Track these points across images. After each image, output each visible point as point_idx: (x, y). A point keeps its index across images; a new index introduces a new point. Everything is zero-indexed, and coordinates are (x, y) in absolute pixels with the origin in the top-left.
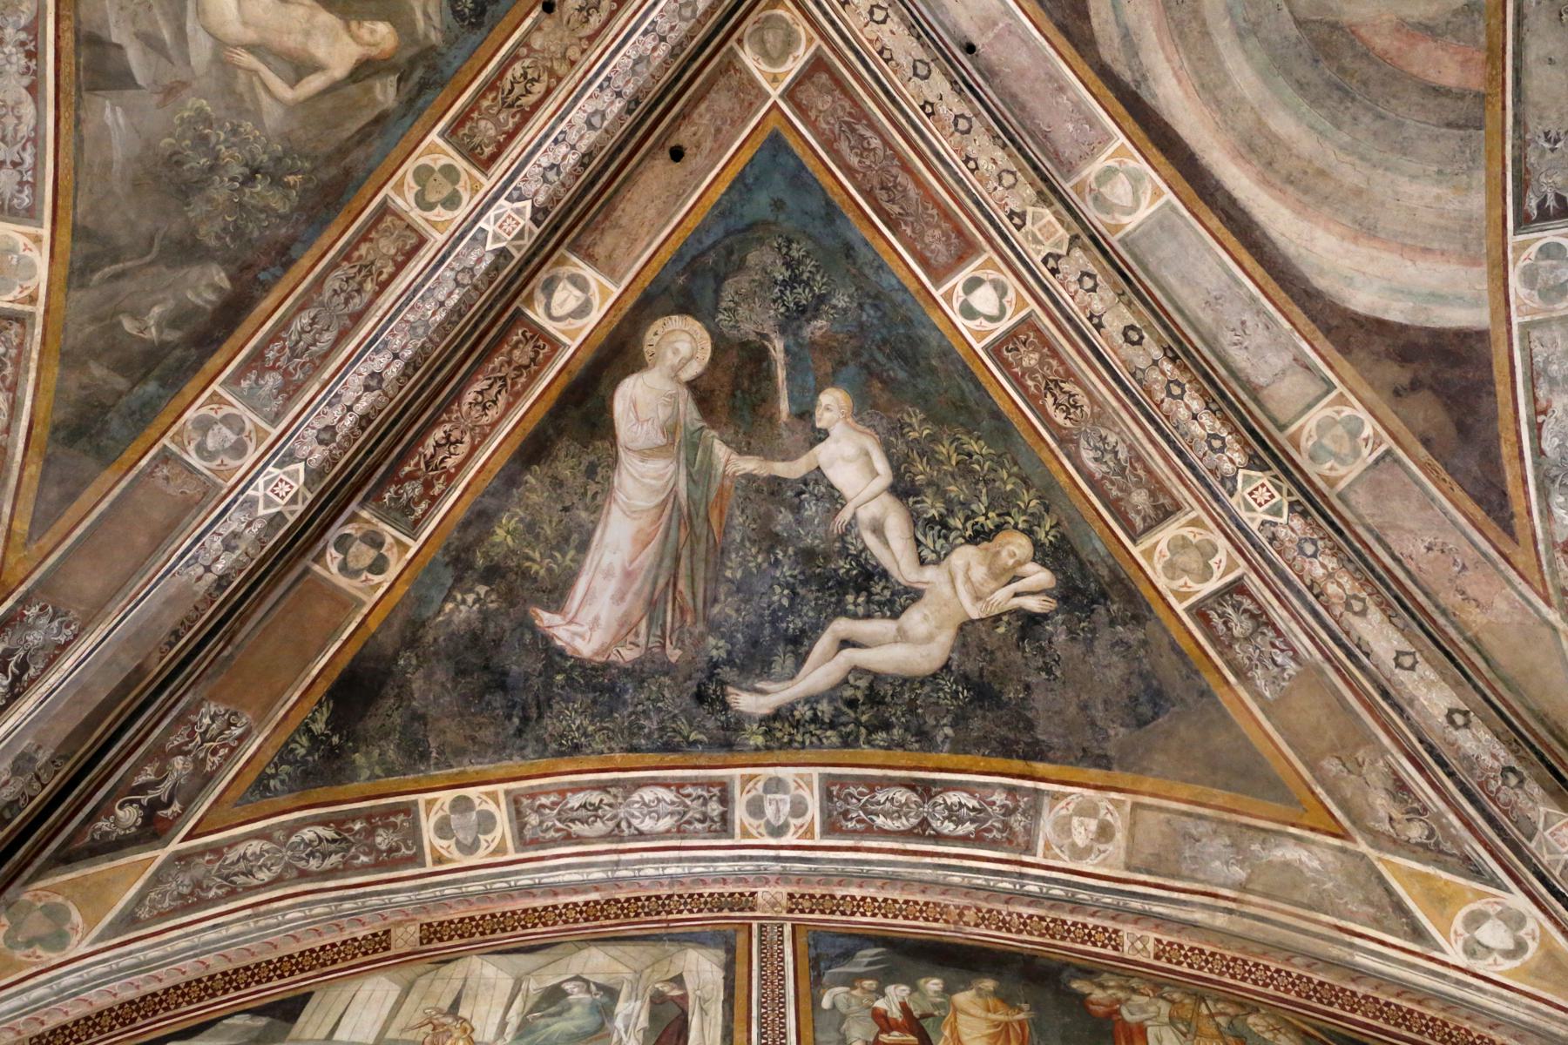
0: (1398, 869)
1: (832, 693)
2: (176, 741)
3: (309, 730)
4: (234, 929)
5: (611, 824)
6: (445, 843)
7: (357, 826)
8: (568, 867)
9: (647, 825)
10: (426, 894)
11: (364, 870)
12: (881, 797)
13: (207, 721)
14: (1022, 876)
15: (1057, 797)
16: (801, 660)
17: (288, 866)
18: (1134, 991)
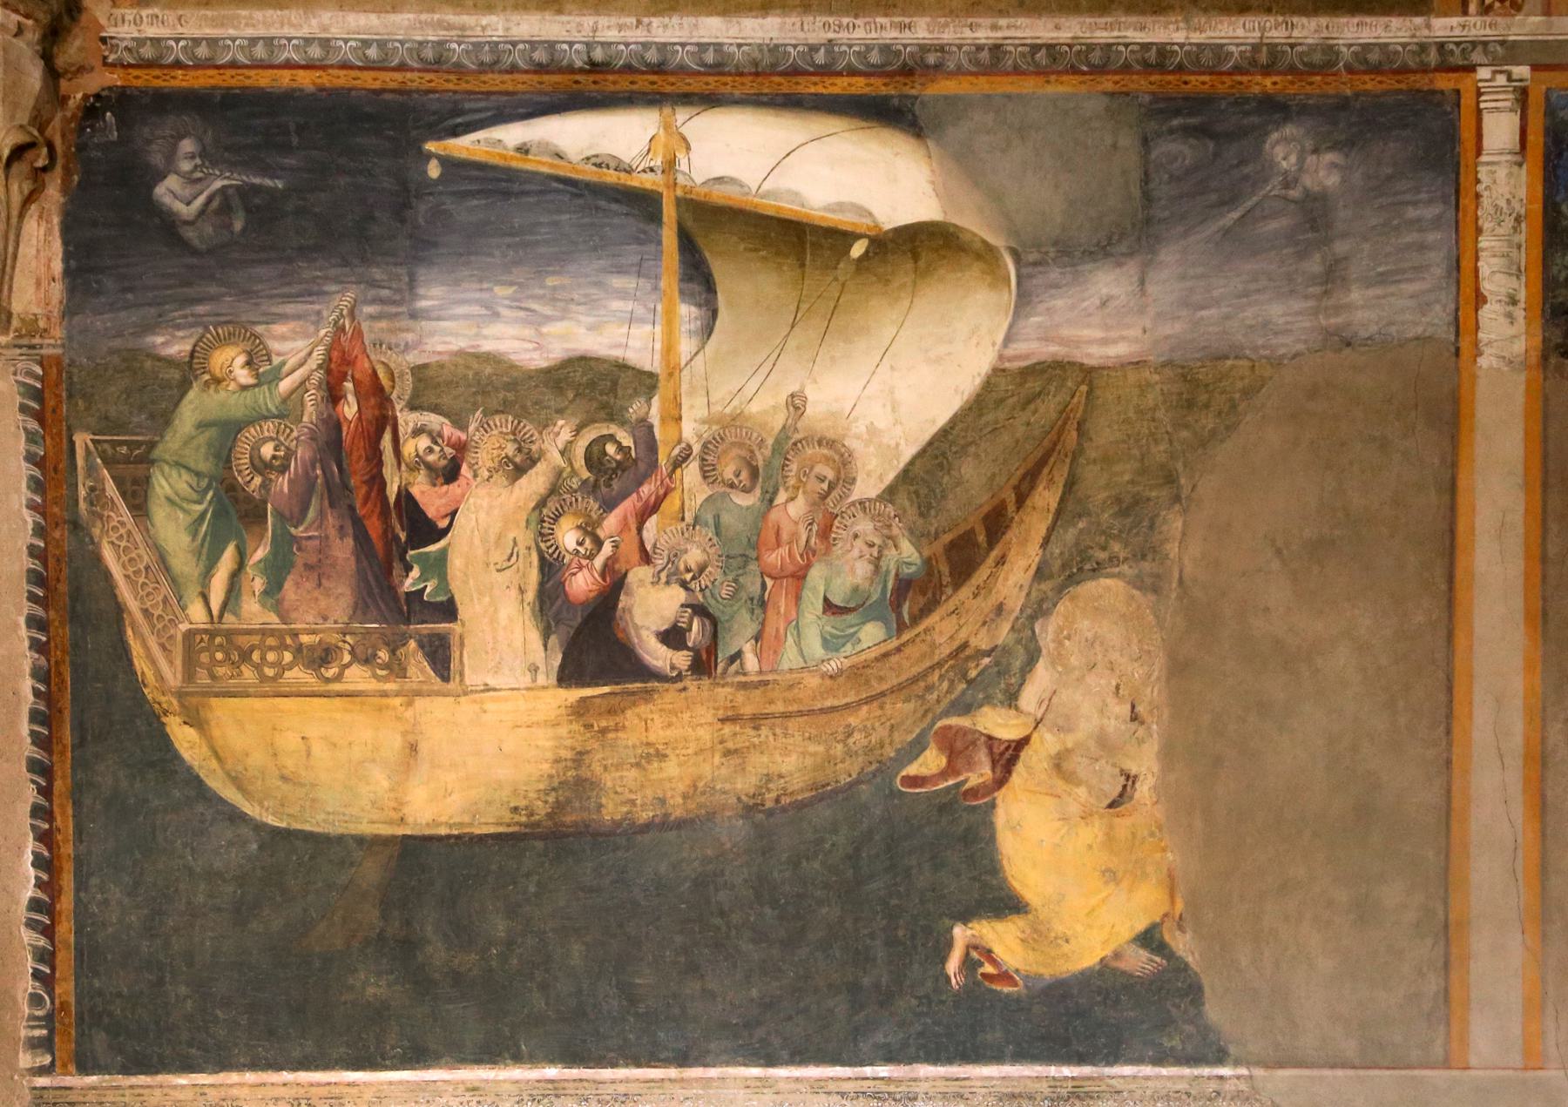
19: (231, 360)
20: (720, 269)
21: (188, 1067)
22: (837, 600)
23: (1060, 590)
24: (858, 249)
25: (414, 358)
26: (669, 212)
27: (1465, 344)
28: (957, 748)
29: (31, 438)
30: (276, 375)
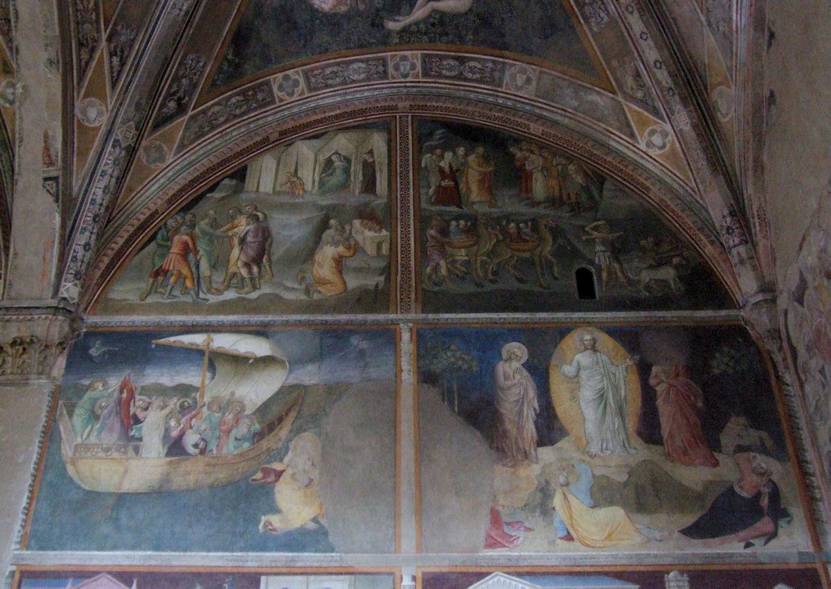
0: (631, 109)
1: (425, 20)
2: (181, 73)
3: (227, 59)
4: (217, 142)
5: (342, 79)
6: (282, 93)
7: (250, 93)
8: (329, 96)
9: (356, 77)
10: (278, 115)
11: (255, 109)
12: (445, 63)
13: (190, 62)
14: (497, 96)
15: (512, 65)
16: (412, 6)
17: (230, 114)
18: (532, 152)
19: (100, 386)
20: (217, 366)
21: (54, 549)
22: (238, 437)
23: (295, 435)
24: (251, 361)
25: (142, 384)
26: (207, 354)
27: (398, 380)
28: (267, 472)
29: (49, 401)
30: (109, 388)
